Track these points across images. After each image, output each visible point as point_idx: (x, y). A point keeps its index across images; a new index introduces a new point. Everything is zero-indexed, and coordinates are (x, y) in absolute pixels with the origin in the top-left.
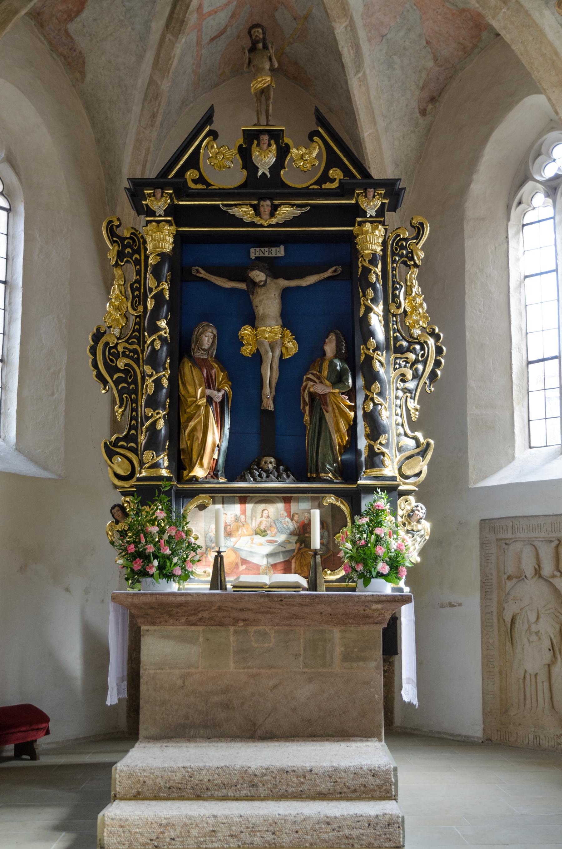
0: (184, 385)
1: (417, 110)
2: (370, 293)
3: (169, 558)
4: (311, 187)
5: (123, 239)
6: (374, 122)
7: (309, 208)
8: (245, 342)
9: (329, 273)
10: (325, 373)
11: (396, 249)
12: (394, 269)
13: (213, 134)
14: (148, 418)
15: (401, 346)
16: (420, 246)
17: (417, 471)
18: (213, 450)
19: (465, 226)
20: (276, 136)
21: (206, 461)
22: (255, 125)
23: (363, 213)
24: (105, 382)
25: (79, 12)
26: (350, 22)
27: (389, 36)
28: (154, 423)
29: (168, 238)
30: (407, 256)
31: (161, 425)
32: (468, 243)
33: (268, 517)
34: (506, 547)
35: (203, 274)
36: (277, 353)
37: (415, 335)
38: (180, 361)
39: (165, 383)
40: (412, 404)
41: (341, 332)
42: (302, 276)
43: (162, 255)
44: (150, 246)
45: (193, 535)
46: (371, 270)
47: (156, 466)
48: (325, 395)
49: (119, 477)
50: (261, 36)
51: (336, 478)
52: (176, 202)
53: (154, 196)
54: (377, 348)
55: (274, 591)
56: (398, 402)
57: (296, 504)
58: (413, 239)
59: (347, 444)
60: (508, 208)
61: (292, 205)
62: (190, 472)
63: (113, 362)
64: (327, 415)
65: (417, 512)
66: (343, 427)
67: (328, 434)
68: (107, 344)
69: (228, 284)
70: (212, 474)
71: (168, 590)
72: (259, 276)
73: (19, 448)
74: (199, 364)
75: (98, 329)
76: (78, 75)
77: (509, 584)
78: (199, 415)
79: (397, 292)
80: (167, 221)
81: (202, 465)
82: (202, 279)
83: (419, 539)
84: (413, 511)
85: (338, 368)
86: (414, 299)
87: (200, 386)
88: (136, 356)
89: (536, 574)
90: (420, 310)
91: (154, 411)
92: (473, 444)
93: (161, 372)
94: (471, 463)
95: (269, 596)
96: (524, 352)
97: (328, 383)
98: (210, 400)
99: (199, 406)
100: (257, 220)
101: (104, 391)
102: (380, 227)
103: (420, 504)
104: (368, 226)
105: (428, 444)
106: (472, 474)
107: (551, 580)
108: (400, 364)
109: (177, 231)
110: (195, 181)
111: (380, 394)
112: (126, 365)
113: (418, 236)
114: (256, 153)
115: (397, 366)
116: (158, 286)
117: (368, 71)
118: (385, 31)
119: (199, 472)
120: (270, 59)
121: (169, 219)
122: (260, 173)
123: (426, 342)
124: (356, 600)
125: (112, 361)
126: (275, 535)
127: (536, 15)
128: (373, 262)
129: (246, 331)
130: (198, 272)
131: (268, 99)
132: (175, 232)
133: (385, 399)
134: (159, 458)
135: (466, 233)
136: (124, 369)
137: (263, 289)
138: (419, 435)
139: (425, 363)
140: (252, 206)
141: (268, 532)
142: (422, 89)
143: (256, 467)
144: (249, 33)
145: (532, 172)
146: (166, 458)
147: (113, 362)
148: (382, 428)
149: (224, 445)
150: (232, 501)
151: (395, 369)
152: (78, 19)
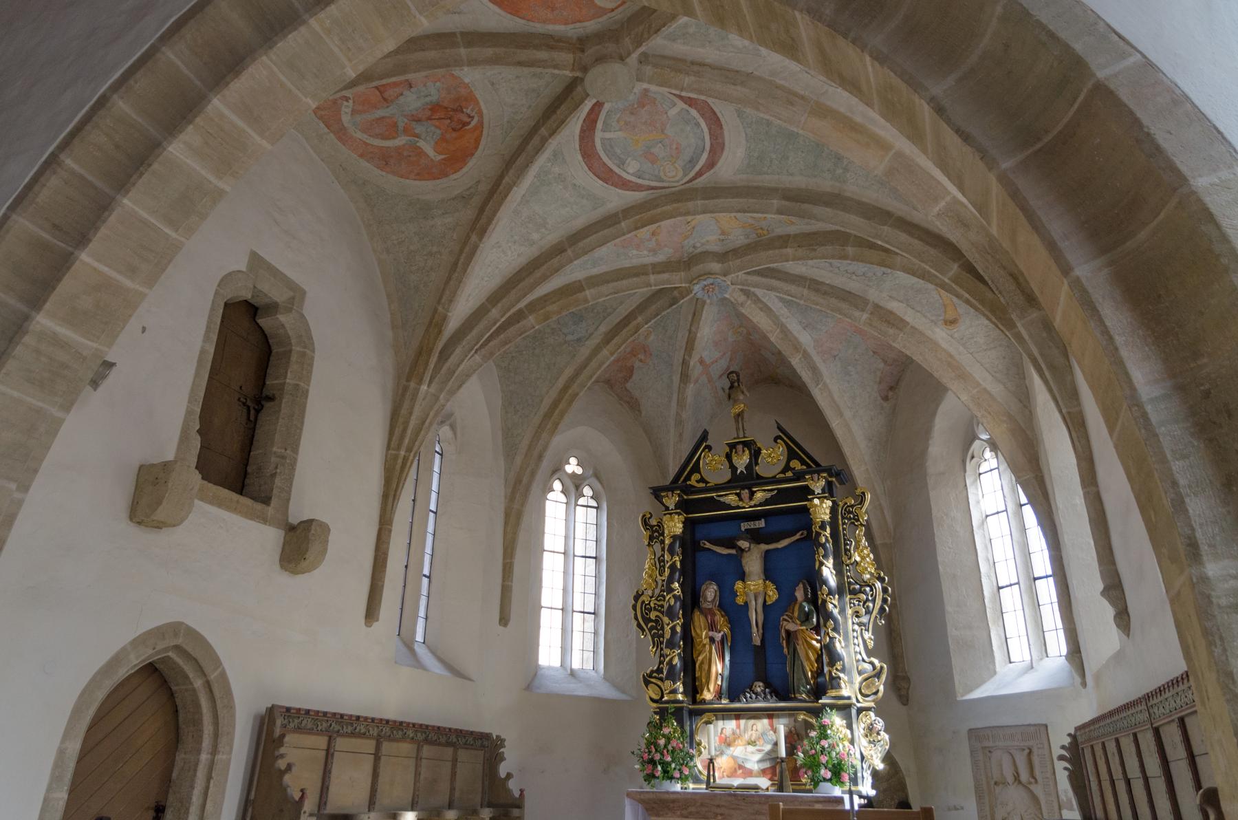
0: (694, 628)
1: (879, 398)
2: (821, 551)
3: (669, 764)
4: (777, 477)
5: (652, 527)
6: (841, 415)
7: (776, 492)
8: (738, 594)
9: (798, 536)
10: (796, 614)
11: (845, 514)
12: (844, 529)
13: (709, 448)
14: (667, 656)
15: (854, 589)
16: (864, 510)
17: (874, 691)
18: (717, 678)
19: (928, 481)
20: (747, 444)
21: (712, 687)
22: (735, 438)
23: (813, 492)
24: (643, 630)
25: (630, 377)
26: (803, 355)
27: (840, 355)
28: (671, 660)
29: (678, 525)
30: (854, 519)
31: (676, 661)
32: (932, 494)
33: (757, 730)
34: (989, 754)
35: (708, 545)
36: (760, 601)
37: (865, 580)
38: (692, 612)
39: (679, 629)
40: (867, 635)
41: (808, 581)
42: (777, 541)
43: (674, 537)
44: (666, 532)
45: (703, 745)
46: (821, 533)
47: (674, 691)
48: (796, 631)
49: (652, 700)
50: (736, 378)
51: (809, 697)
52: (685, 497)
53: (667, 496)
54: (830, 593)
55: (739, 792)
56: (855, 634)
57: (777, 720)
58: (858, 505)
59: (817, 670)
60: (964, 462)
61: (765, 490)
62: (701, 695)
64: (798, 647)
65: (875, 725)
66: (812, 657)
67: (800, 662)
68: (643, 602)
69: (725, 551)
70: (717, 696)
71: (673, 789)
72: (744, 544)
73: (607, 677)
74: (705, 613)
75: (637, 592)
76: (637, 412)
77: (998, 789)
78: (705, 651)
79: (848, 547)
80: (676, 513)
81: (709, 690)
82: (709, 549)
83: (880, 749)
84: (872, 724)
85: (807, 609)
86: (862, 551)
87: (705, 629)
89: (1016, 779)
90: (868, 559)
91: (671, 650)
92: (956, 662)
93: (676, 621)
94: (957, 678)
95: (735, 795)
96: (994, 579)
97: (798, 622)
98: (712, 640)
99: (704, 645)
100: (740, 504)
101: (642, 637)
102: (825, 500)
103: (878, 718)
104: (816, 501)
105: (882, 668)
106: (959, 688)
107: (1028, 786)
108: (854, 604)
109: (686, 518)
110: (698, 482)
111: (835, 629)
112: (656, 617)
113: (862, 502)
114: (735, 459)
115: (852, 605)
116: (672, 559)
117: (828, 381)
118: (836, 353)
119: (708, 695)
120: (743, 392)
121: (678, 511)
122: (739, 472)
123: (874, 585)
124: (800, 800)
125: (647, 614)
126: (762, 746)
127: (929, 333)
128: (823, 527)
129: (739, 585)
130: (705, 544)
132: (683, 520)
133: (839, 633)
134: (676, 686)
135: (930, 487)
137: (748, 553)
138: (876, 662)
139: (874, 601)
140: (736, 494)
141: (758, 743)
142: (880, 383)
143: (748, 690)
144: (728, 377)
145: (977, 432)
146: (681, 685)
148: (837, 656)
149: (727, 673)
150: (729, 718)
151: (851, 607)
152: (631, 380)
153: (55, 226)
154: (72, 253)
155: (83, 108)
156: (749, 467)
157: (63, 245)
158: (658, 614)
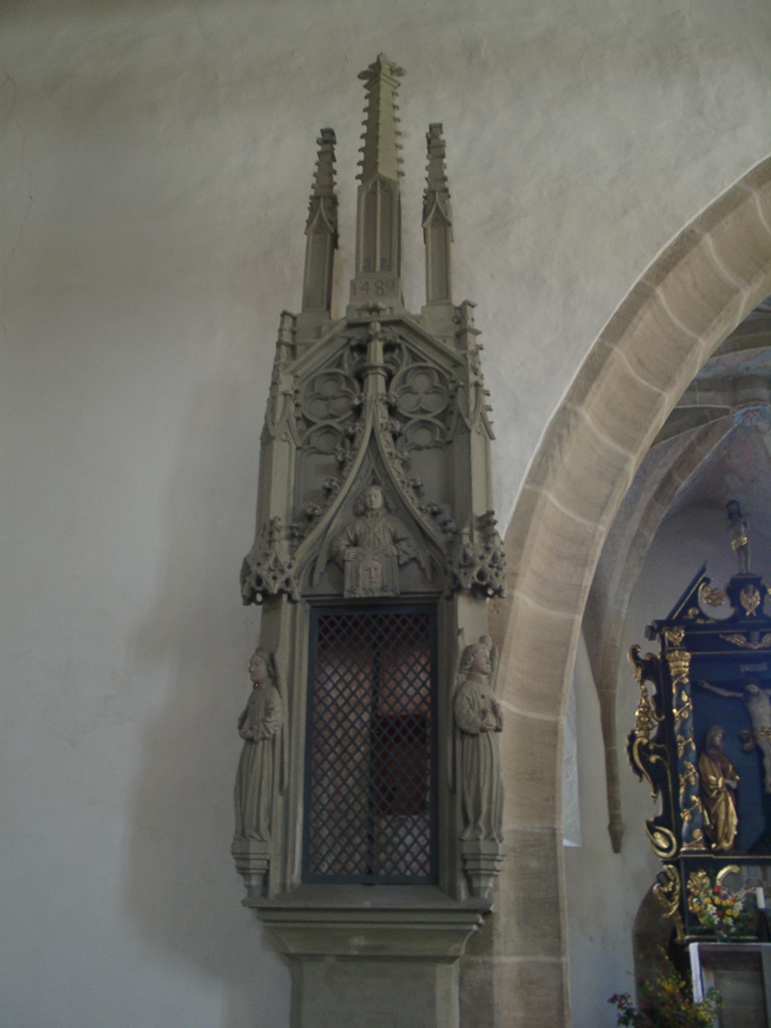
35: (706, 685)
110: (696, 617)
114: (743, 596)
131: (746, 554)
153: (640, 362)
154: (659, 395)
155: (668, 239)
156: (759, 609)
157: (646, 383)
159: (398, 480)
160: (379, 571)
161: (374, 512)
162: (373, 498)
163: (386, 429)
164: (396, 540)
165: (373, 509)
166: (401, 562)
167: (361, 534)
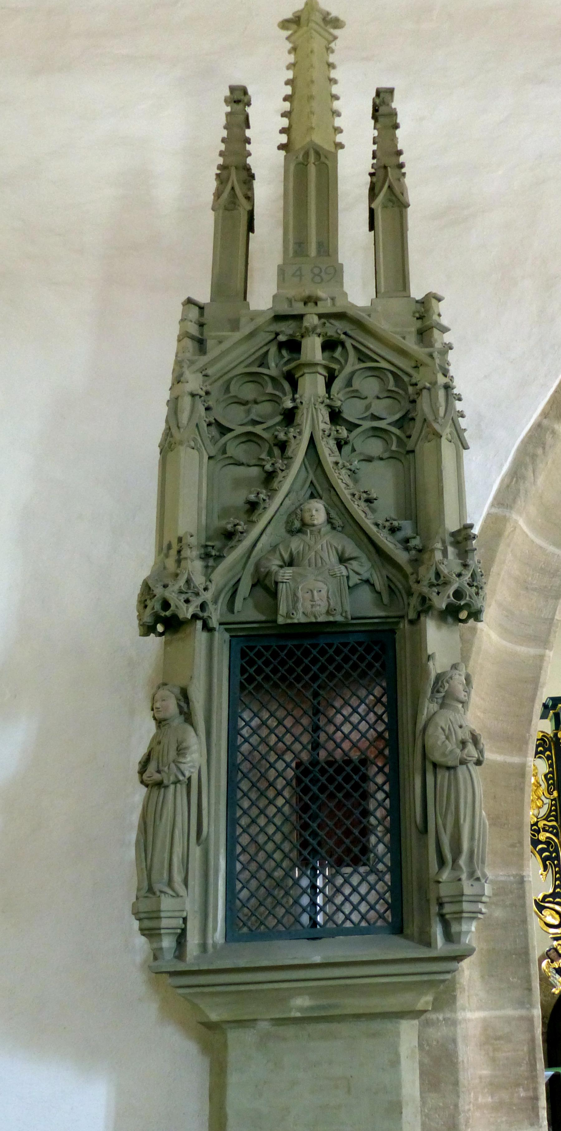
63: (535, 836)
88: (555, 831)
136: (546, 841)
147: (535, 836)
158: (548, 835)
159: (346, 492)
160: (324, 593)
161: (313, 528)
162: (314, 512)
163: (329, 436)
164: (343, 560)
165: (314, 525)
166: (351, 584)
167: (298, 553)
